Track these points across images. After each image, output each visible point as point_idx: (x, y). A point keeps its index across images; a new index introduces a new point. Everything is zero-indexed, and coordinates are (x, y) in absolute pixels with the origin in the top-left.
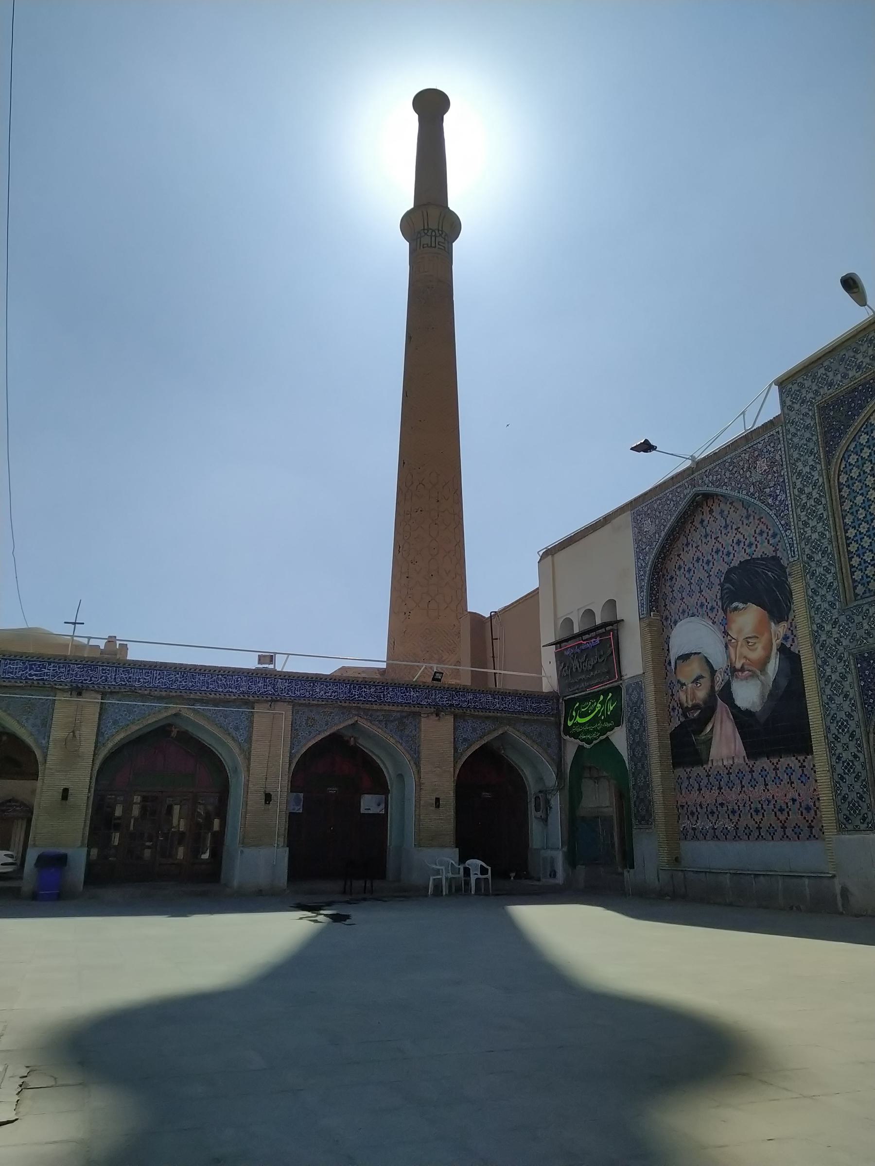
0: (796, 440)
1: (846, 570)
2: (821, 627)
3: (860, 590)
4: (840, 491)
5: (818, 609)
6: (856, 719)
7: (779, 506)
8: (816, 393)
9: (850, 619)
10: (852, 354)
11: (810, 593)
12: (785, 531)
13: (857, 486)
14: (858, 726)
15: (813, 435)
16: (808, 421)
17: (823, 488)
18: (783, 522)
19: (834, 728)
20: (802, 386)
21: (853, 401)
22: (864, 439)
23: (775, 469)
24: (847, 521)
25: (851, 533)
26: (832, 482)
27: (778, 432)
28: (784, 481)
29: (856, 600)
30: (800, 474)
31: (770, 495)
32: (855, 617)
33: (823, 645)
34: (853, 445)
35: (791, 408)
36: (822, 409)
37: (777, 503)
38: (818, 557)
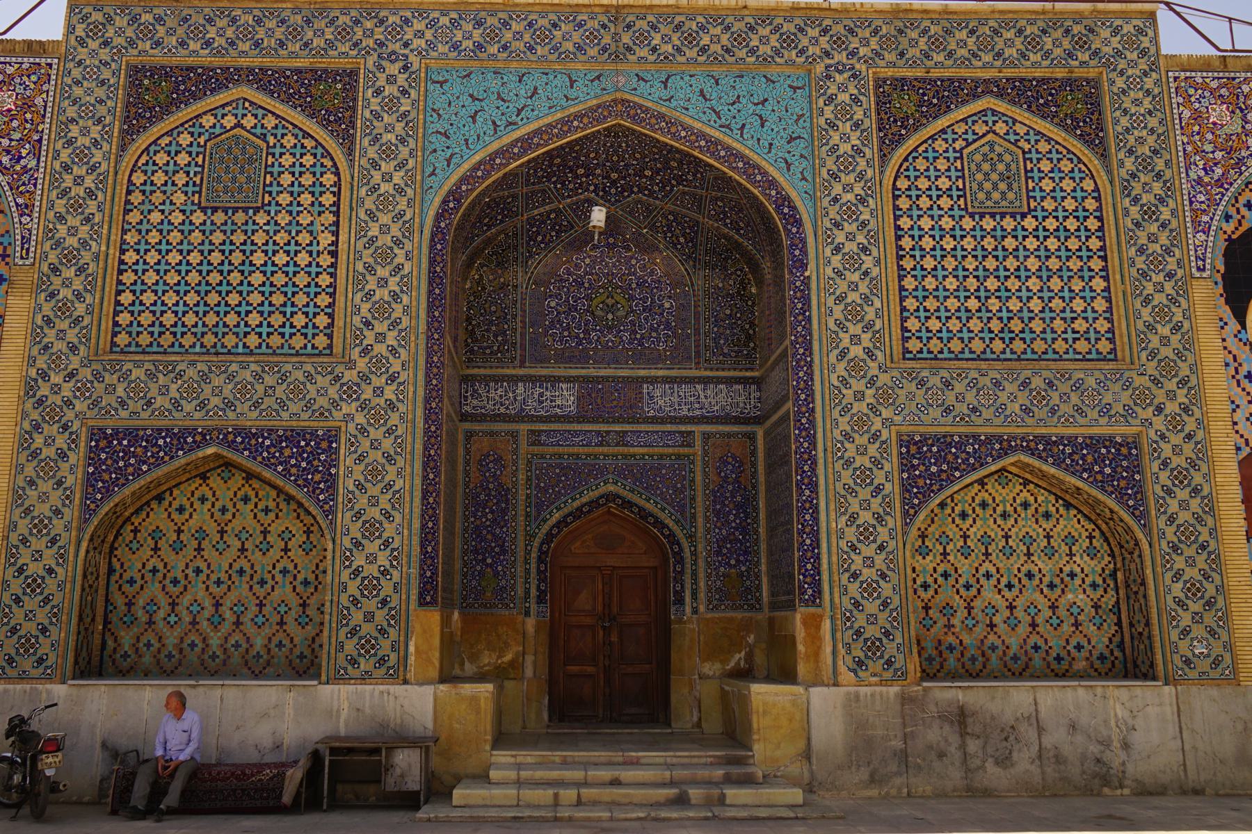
0: (78, 92)
1: (109, 308)
2: (44, 375)
3: (122, 339)
4: (129, 192)
5: (46, 348)
6: (67, 518)
7: (20, 174)
8: (132, 43)
9: (98, 376)
10: (202, 21)
11: (39, 321)
12: (21, 215)
13: (158, 197)
14: (67, 528)
15: (109, 97)
16: (106, 74)
17: (106, 178)
18: (20, 201)
19: (23, 526)
20: (110, 20)
21: (184, 82)
22: (185, 139)
23: (28, 116)
24: (128, 237)
25: (131, 257)
26: (119, 176)
27: (50, 65)
28: (40, 141)
29: (111, 352)
30: (70, 142)
31: (8, 152)
32: (107, 375)
33: (40, 402)
34: (166, 140)
35: (82, 42)
36: (136, 72)
37: (18, 168)
38: (69, 273)
